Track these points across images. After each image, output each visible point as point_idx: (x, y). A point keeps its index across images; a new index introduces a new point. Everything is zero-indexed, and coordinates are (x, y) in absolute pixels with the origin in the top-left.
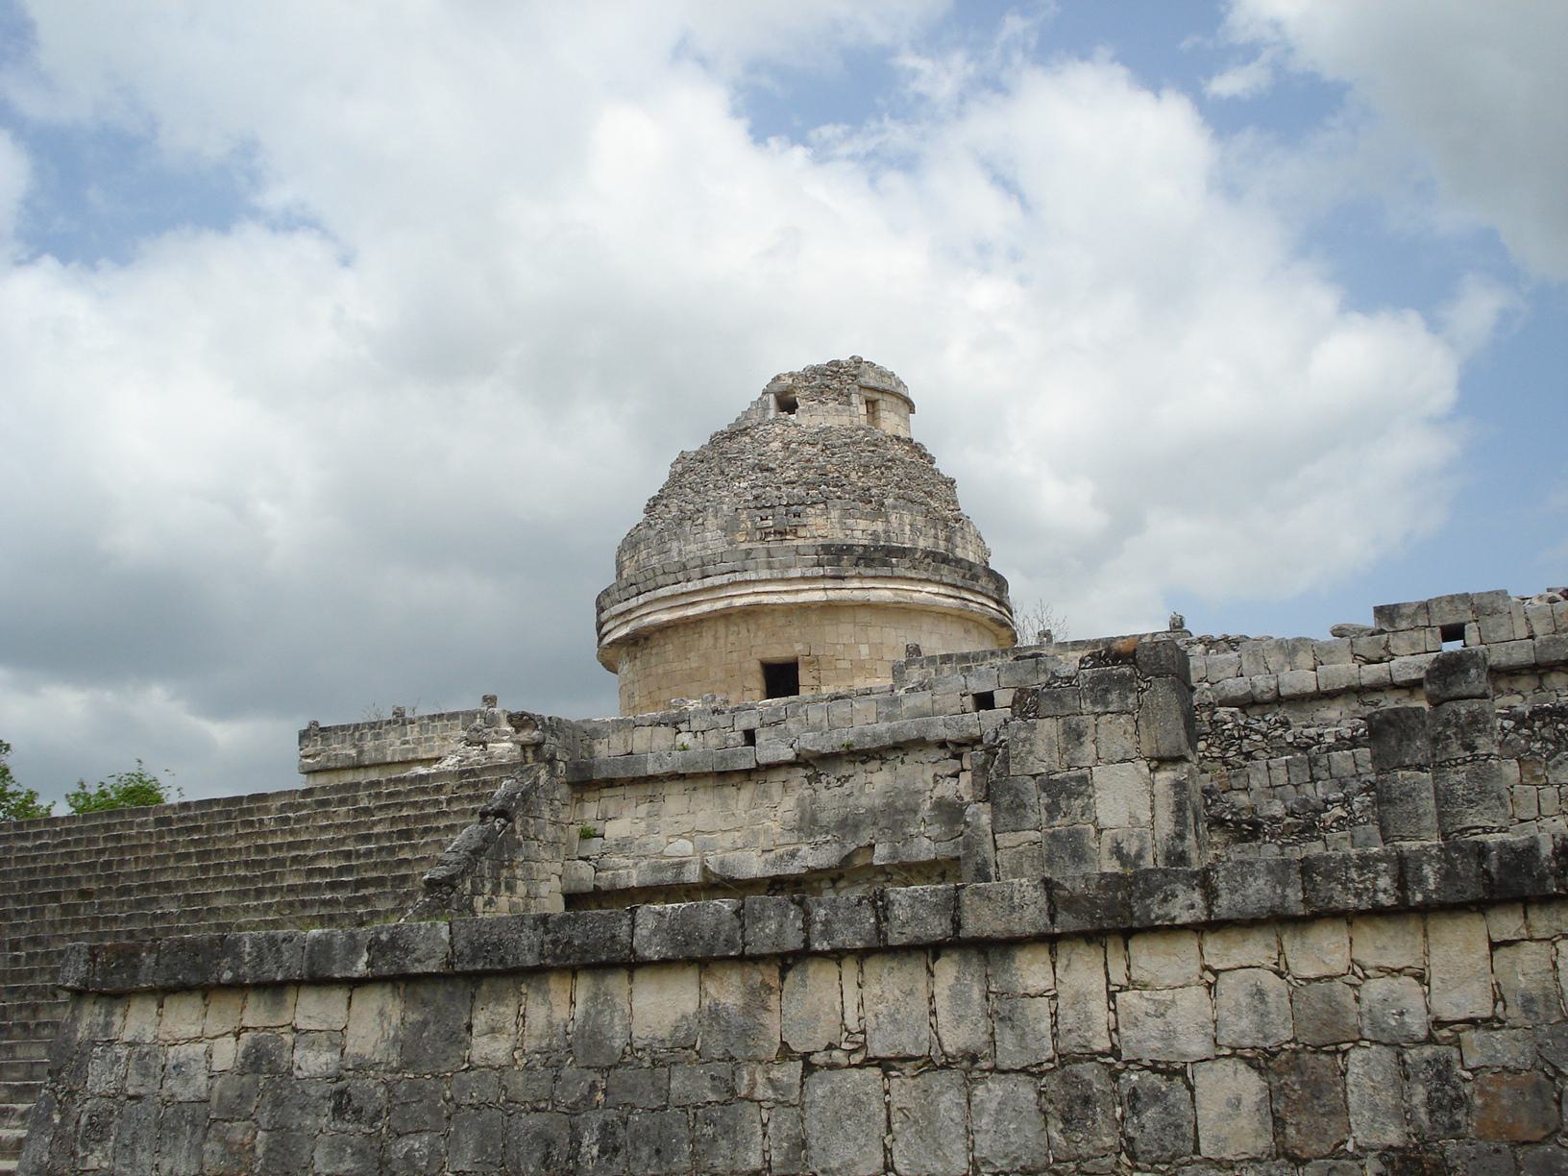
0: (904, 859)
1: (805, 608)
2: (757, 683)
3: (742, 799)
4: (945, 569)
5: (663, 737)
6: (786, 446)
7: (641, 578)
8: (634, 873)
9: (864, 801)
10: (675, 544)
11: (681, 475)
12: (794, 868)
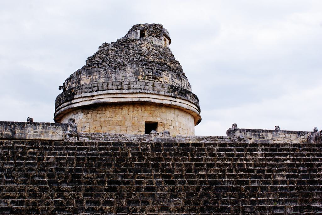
1: (161, 106)
2: (143, 129)
7: (100, 85)
10: (113, 75)
11: (108, 50)
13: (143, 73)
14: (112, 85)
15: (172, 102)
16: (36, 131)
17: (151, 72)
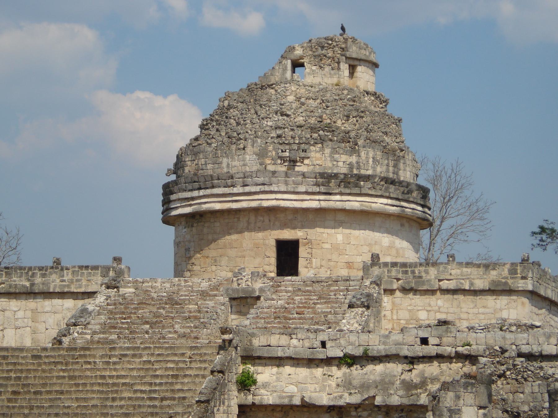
0: (388, 403)
3: (319, 372)
4: (392, 188)
5: (284, 340)
6: (298, 99)
7: (202, 180)
8: (271, 398)
9: (372, 377)
10: (225, 160)
11: (230, 107)
12: (341, 403)
13: (274, 153)
14: (219, 179)
15: (321, 202)
16: (64, 279)
17: (288, 151)
